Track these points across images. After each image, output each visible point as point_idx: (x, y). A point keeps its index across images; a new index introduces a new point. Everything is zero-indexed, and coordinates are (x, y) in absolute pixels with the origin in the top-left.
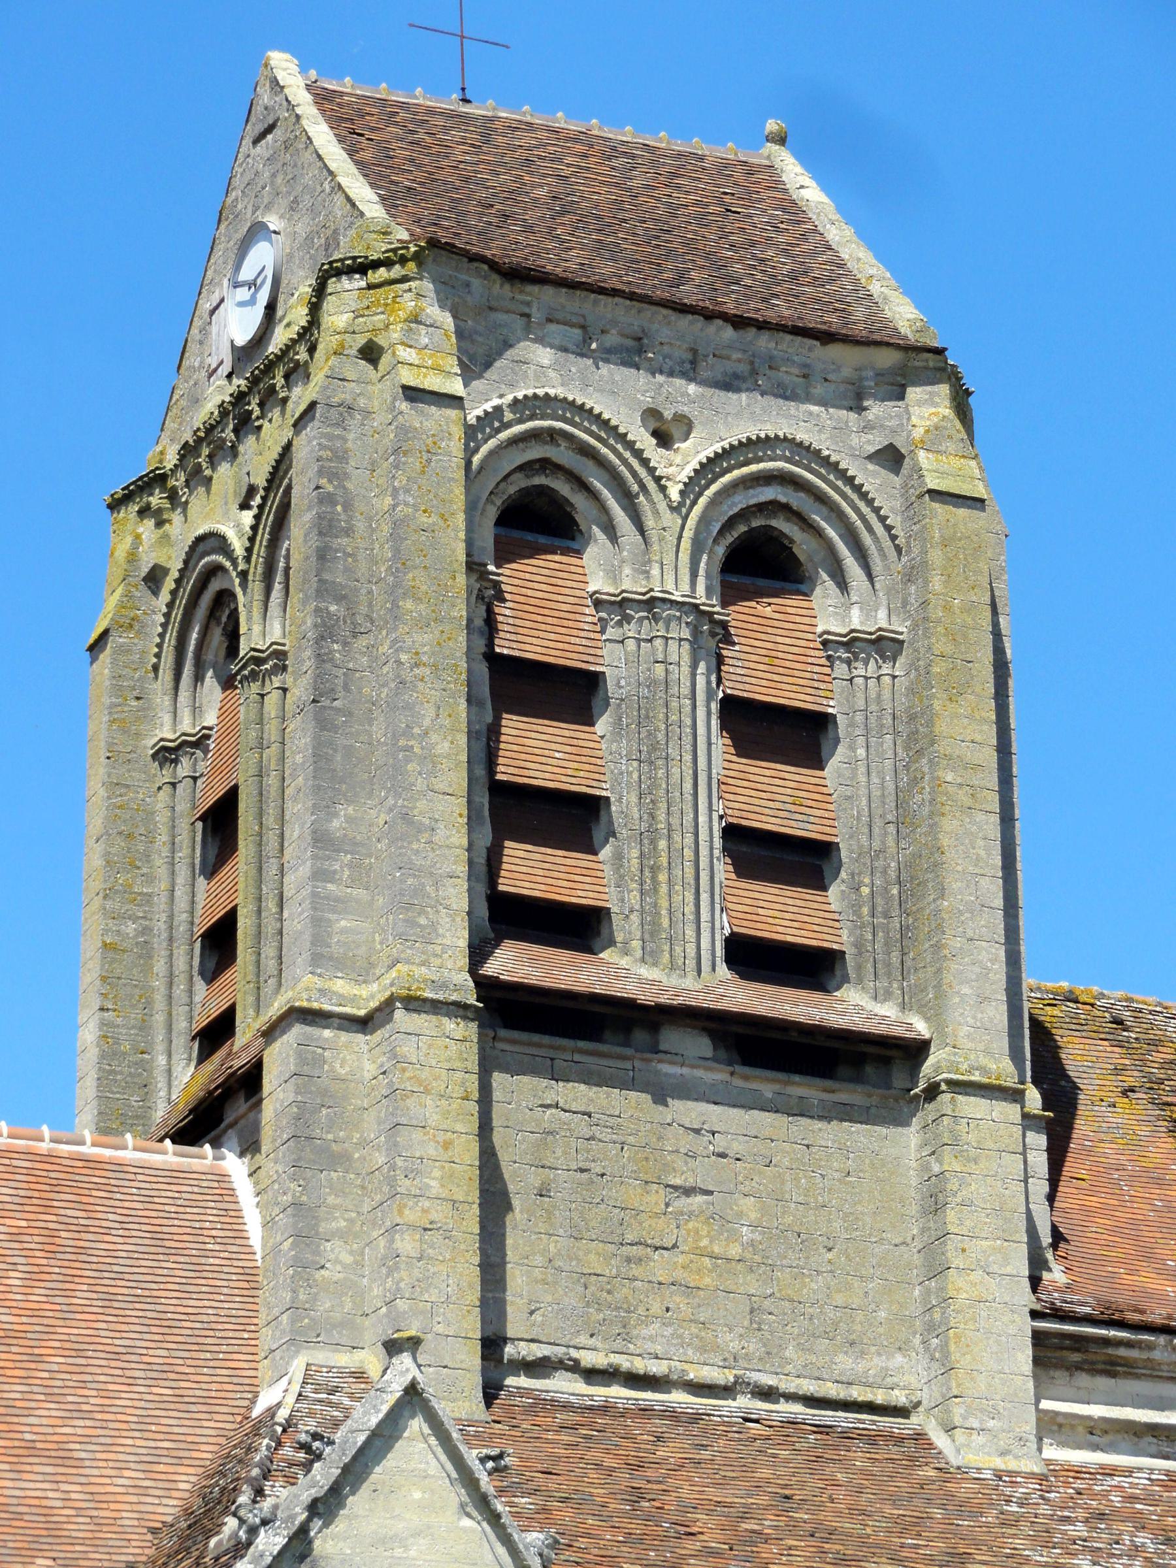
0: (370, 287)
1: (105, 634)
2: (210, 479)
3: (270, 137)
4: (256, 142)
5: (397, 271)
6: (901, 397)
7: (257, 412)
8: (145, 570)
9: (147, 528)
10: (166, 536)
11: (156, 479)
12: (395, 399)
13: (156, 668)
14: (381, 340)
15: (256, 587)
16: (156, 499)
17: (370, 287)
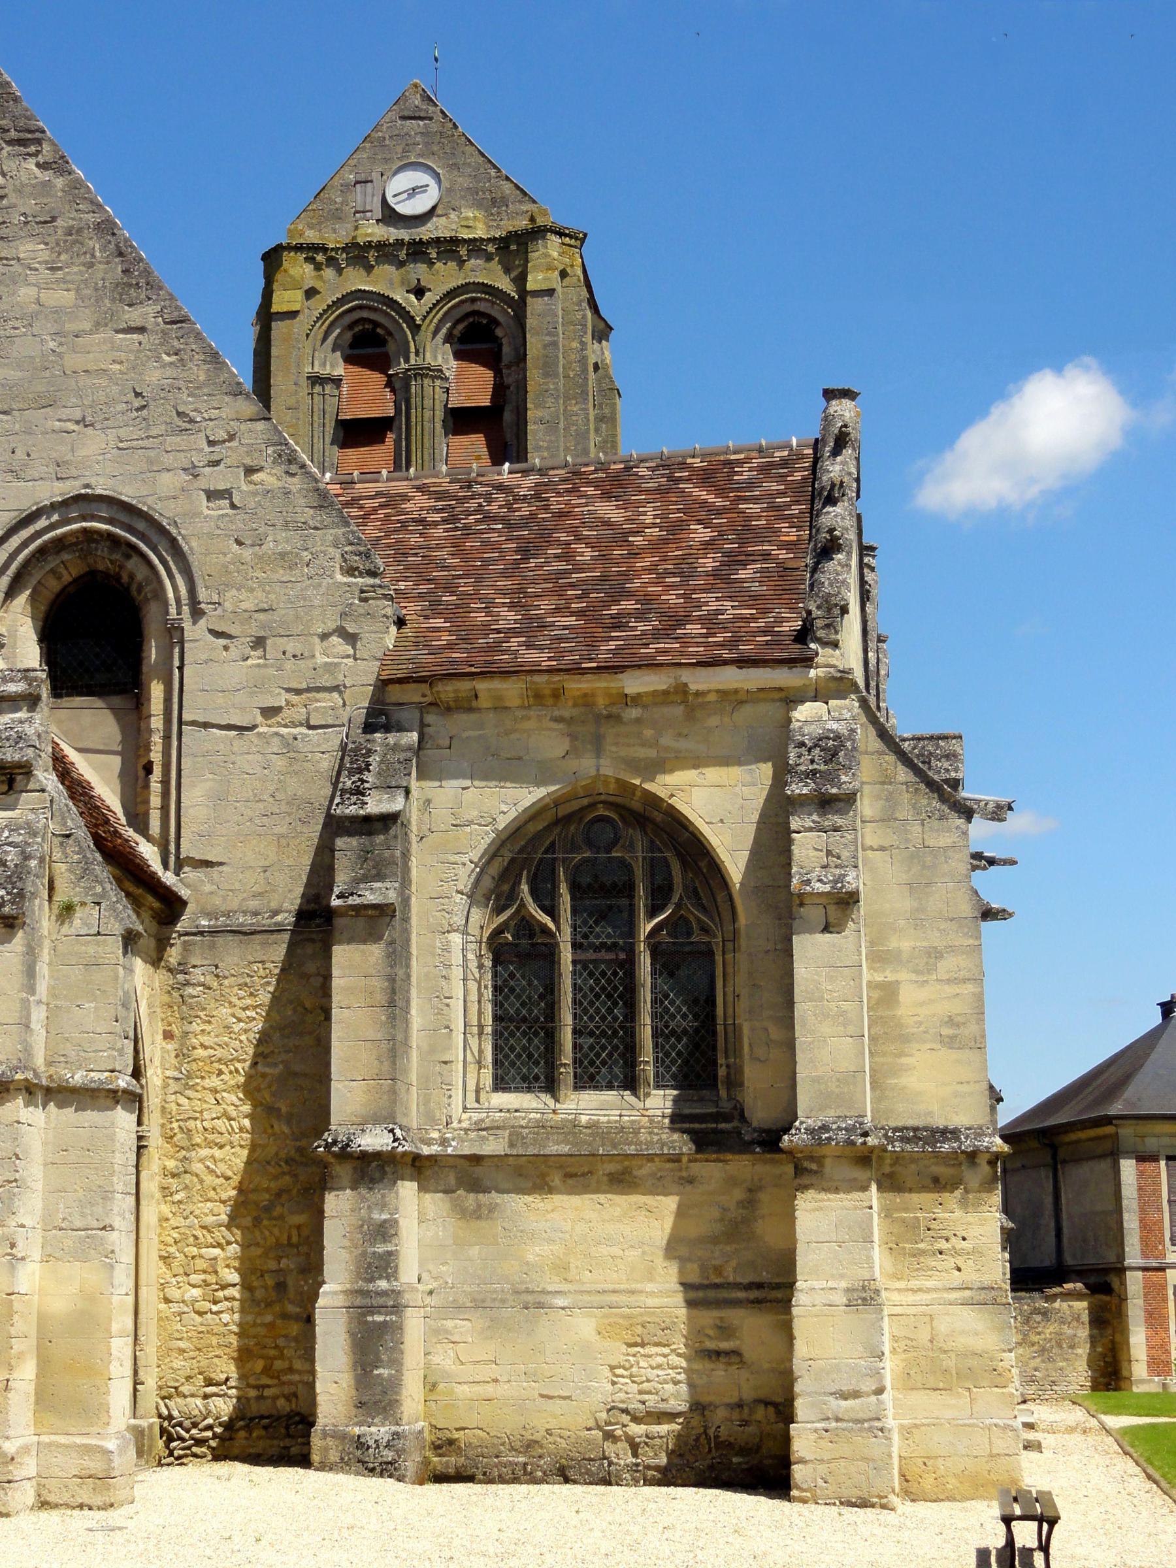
0: (563, 244)
1: (297, 312)
2: (373, 267)
3: (421, 123)
4: (403, 118)
5: (573, 242)
6: (600, 342)
7: (434, 255)
8: (306, 287)
9: (308, 268)
10: (321, 277)
11: (323, 249)
12: (581, 301)
13: (308, 335)
14: (569, 270)
15: (430, 335)
16: (320, 258)
17: (563, 244)
